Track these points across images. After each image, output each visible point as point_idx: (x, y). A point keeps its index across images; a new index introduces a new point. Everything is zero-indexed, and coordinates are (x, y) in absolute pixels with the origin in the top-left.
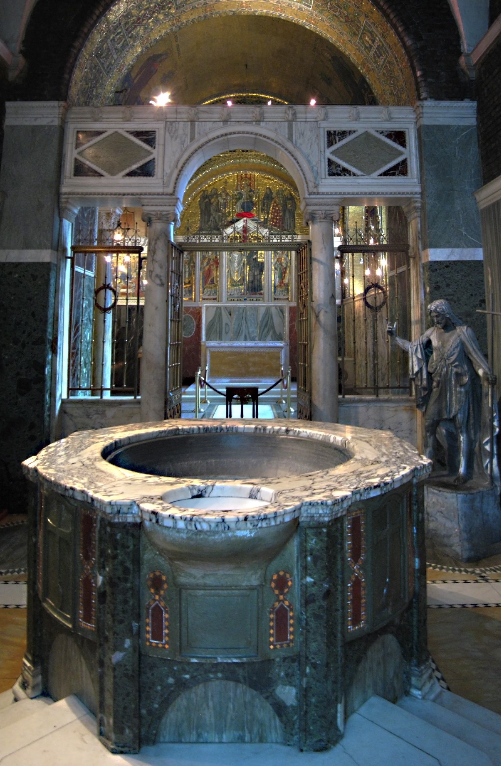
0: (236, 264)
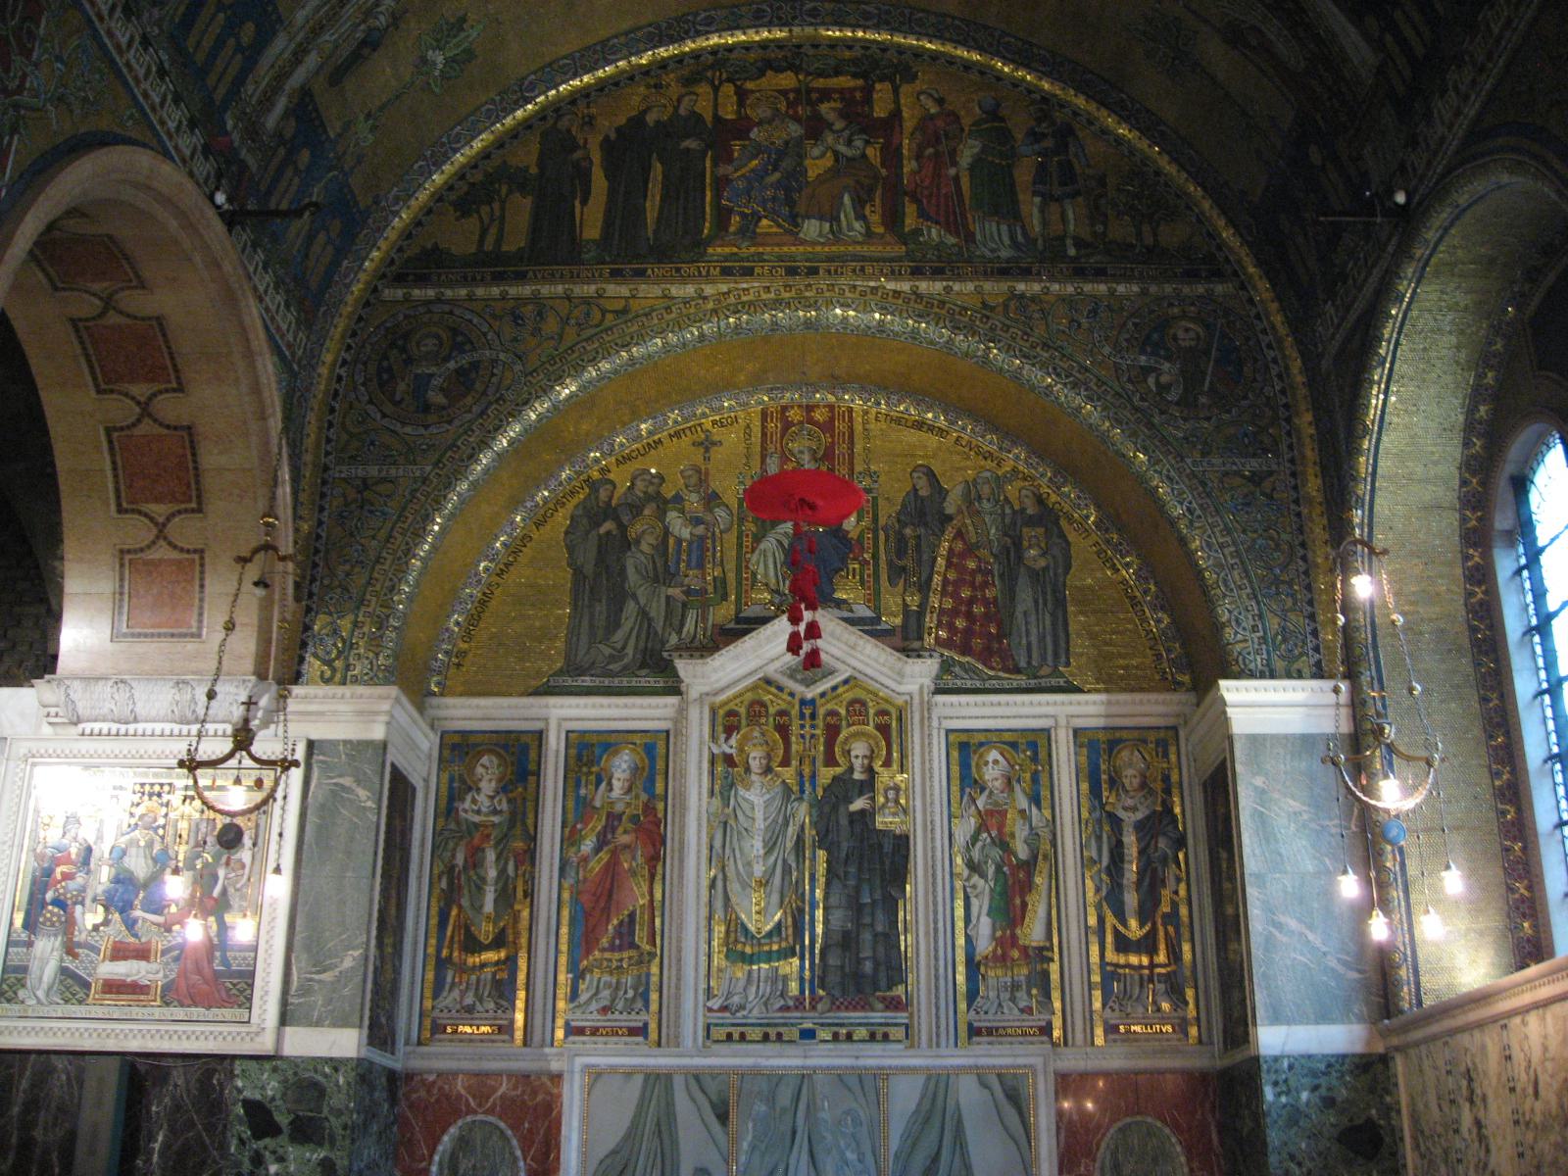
0: (757, 846)
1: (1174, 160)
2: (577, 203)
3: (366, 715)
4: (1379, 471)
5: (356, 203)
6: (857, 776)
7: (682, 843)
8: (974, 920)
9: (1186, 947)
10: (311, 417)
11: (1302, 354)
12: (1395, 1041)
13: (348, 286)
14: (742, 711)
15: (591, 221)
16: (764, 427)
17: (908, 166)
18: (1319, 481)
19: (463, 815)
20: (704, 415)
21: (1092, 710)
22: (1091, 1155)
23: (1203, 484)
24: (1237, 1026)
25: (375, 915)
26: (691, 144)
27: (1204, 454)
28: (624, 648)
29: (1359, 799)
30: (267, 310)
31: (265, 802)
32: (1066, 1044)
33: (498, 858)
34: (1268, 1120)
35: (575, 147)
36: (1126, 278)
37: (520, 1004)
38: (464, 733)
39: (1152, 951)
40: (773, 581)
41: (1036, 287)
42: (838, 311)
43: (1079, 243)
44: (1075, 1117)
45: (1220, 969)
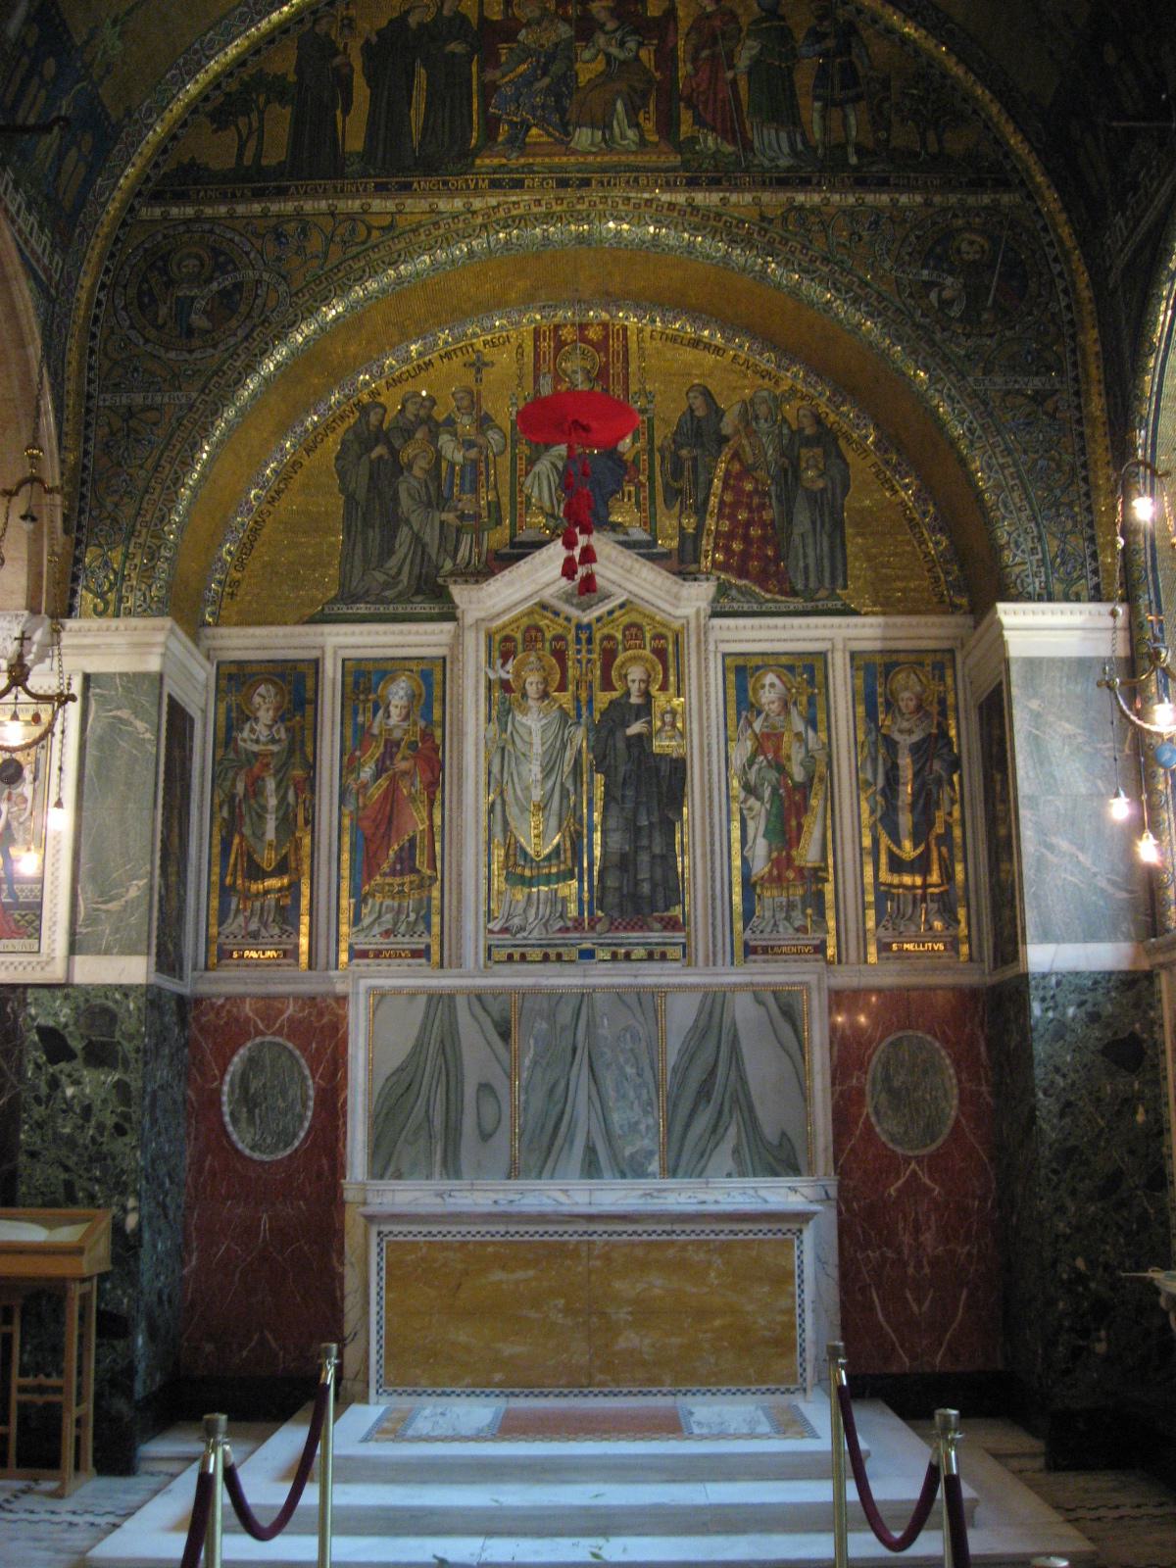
0: (535, 770)
1: (961, 60)
2: (338, 112)
3: (142, 648)
4: (1165, 390)
5: (108, 117)
6: (634, 700)
7: (460, 769)
8: (750, 844)
9: (959, 868)
10: (72, 343)
11: (1089, 268)
12: (1160, 958)
13: (104, 205)
14: (519, 636)
15: (353, 131)
16: (536, 347)
17: (684, 69)
18: (1103, 400)
19: (241, 743)
20: (475, 335)
21: (868, 632)
22: (862, 1065)
23: (985, 403)
24: (1007, 942)
25: (158, 845)
26: (456, 47)
27: (987, 372)
28: (399, 573)
29: (1132, 723)
30: (20, 231)
31: (43, 737)
32: (840, 962)
33: (278, 786)
34: (1035, 1035)
35: (336, 53)
36: (910, 188)
37: (304, 929)
38: (240, 663)
39: (925, 871)
40: (547, 504)
41: (816, 198)
42: (611, 225)
43: (860, 151)
44: (848, 1032)
45: (992, 889)
